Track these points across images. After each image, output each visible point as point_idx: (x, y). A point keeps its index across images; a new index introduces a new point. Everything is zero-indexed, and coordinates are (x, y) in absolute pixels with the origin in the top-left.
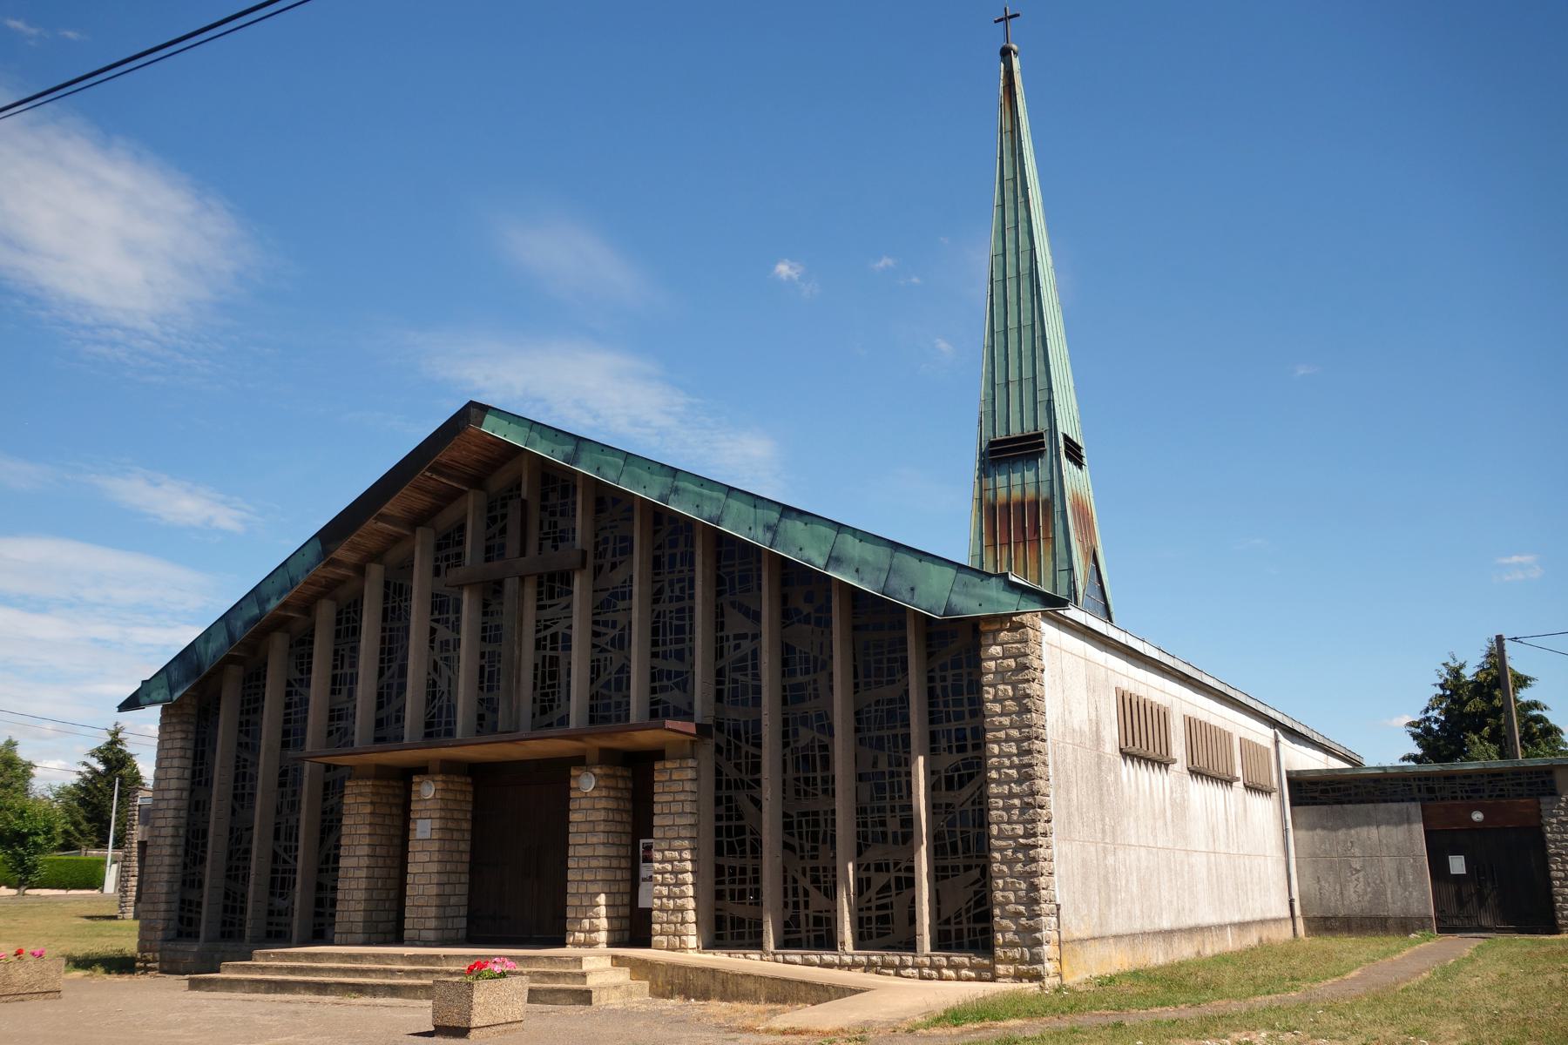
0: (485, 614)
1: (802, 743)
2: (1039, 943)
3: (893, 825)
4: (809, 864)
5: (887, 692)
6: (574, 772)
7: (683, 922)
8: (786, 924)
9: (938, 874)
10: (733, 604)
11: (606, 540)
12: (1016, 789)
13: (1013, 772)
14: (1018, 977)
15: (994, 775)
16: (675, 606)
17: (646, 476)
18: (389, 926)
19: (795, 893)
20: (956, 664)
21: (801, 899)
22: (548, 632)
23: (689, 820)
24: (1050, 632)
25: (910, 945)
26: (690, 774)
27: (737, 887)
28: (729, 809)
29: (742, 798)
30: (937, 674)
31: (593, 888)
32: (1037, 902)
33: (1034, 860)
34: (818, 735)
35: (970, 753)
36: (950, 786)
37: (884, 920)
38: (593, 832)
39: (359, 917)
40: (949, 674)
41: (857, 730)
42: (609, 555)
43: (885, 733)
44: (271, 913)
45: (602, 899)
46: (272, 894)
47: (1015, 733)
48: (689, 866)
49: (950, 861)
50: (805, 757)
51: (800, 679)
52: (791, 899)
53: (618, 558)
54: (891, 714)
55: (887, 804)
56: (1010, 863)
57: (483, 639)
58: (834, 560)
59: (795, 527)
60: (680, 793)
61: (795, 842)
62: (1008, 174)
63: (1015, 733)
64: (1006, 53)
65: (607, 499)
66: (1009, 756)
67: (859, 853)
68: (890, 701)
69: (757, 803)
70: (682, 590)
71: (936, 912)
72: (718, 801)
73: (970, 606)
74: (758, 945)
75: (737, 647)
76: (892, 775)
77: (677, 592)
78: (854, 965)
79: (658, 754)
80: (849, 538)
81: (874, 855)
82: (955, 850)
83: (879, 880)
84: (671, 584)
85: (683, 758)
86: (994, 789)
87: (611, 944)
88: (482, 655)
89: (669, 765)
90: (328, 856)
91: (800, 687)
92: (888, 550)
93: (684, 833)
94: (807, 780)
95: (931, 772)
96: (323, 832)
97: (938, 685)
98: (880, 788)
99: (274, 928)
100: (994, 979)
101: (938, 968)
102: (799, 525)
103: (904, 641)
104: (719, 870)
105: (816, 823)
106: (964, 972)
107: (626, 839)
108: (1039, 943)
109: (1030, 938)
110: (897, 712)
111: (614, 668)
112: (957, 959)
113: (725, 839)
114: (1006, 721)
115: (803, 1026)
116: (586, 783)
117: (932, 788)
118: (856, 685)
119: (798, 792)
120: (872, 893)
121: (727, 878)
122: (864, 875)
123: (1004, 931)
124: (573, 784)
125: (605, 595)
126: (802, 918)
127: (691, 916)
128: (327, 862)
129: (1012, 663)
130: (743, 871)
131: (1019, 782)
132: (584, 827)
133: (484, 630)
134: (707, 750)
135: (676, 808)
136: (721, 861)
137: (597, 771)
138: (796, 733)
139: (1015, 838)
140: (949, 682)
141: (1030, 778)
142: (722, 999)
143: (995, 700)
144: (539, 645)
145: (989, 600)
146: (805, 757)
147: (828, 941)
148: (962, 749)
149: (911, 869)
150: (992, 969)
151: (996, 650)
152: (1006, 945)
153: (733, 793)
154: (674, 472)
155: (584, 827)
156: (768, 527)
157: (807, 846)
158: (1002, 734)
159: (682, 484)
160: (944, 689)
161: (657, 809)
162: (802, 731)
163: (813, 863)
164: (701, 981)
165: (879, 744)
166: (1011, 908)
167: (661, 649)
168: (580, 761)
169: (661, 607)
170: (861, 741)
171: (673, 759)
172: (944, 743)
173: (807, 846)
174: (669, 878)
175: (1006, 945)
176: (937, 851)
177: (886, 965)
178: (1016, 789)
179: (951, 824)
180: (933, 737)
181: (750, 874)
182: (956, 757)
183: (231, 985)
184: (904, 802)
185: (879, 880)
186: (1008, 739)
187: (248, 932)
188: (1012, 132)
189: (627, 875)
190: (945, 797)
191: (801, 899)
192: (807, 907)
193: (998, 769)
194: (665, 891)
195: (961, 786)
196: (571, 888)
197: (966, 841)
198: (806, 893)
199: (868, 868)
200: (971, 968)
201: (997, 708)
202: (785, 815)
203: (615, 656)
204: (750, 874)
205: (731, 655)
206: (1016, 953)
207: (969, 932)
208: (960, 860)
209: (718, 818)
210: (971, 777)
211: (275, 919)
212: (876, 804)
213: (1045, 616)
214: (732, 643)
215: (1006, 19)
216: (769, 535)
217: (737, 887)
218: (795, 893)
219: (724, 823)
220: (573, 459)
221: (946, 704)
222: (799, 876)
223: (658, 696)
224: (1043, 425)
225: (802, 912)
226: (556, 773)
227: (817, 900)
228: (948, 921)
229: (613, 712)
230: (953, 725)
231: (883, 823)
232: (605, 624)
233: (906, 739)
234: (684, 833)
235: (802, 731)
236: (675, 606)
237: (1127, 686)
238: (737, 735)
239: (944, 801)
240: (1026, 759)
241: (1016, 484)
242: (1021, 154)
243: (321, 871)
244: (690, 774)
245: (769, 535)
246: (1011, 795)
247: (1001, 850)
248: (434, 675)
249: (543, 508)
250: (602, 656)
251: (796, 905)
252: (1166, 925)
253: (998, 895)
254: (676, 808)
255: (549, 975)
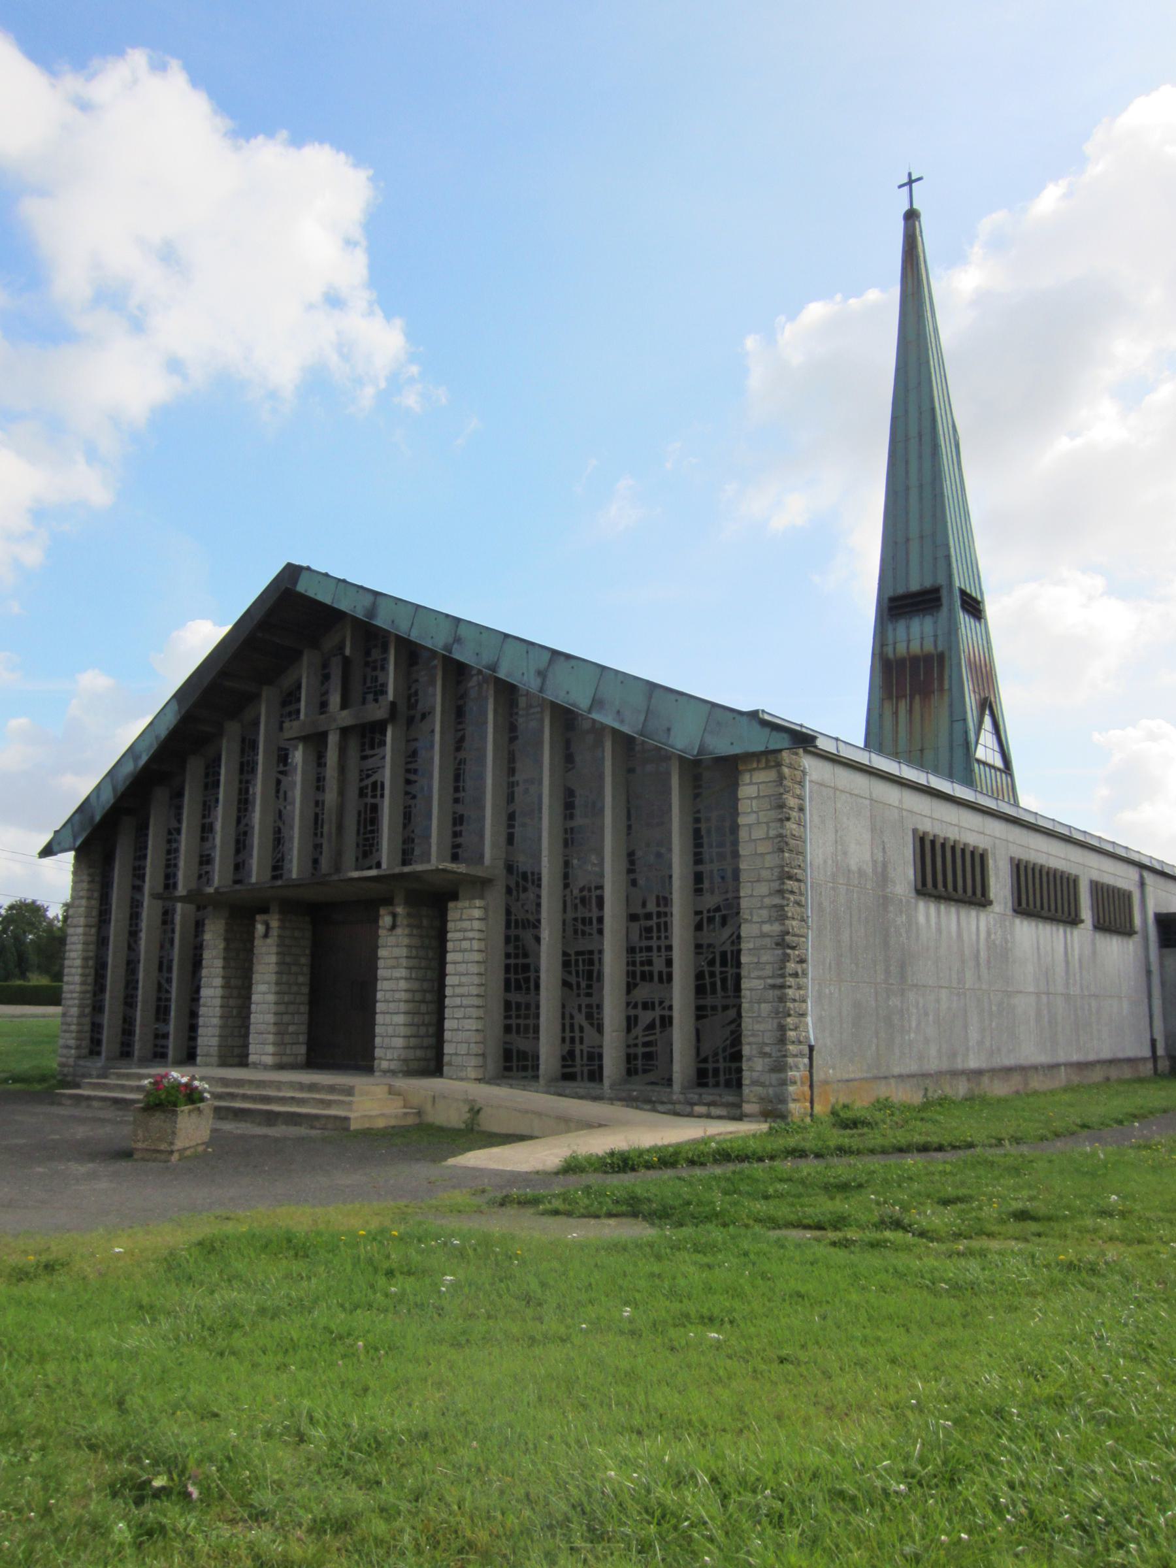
4: (585, 1001)
19: (572, 1030)
23: (477, 957)
26: (477, 913)
28: (516, 947)
29: (527, 936)
37: (648, 1056)
49: (709, 1001)
52: (568, 1034)
55: (654, 943)
60: (471, 933)
61: (573, 980)
69: (538, 939)
72: (508, 940)
76: (659, 915)
82: (714, 992)
83: (646, 1017)
104: (508, 1005)
119: (576, 932)
120: (638, 1031)
121: (513, 1013)
122: (632, 1012)
126: (578, 1052)
144: (362, 793)
157: (583, 984)
173: (583, 984)
179: (711, 963)
185: (646, 1017)
191: (577, 1034)
192: (581, 1042)
197: (724, 981)
198: (581, 1029)
202: (565, 954)
207: (719, 1074)
209: (508, 956)
212: (644, 943)
218: (572, 1030)
222: (575, 1012)
224: (941, 580)
228: (705, 1060)
231: (650, 963)
237: (926, 826)
239: (705, 942)
241: (917, 634)
244: (477, 913)
245: (539, 681)
251: (572, 1040)
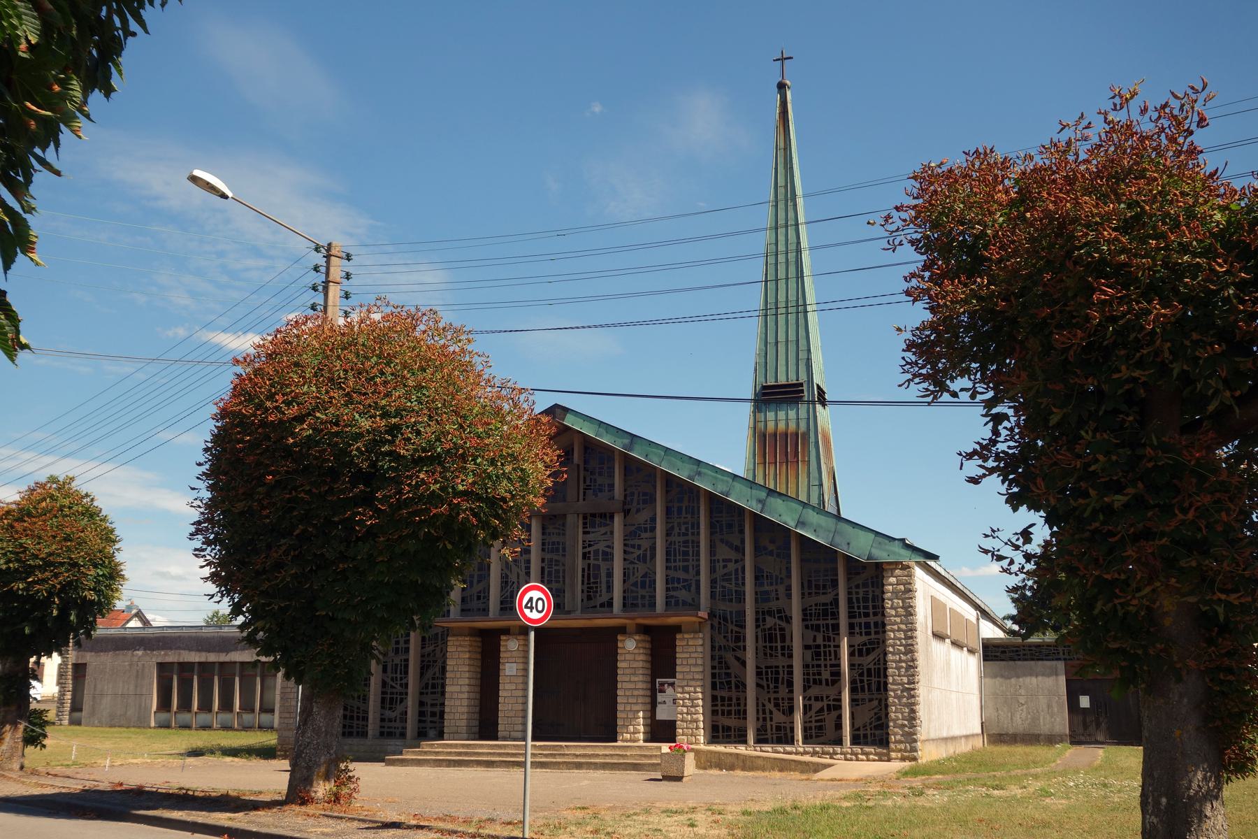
0: (543, 534)
1: (768, 626)
2: (915, 741)
3: (826, 675)
4: (773, 696)
5: (823, 599)
6: (620, 637)
7: (697, 728)
8: (758, 730)
9: (853, 701)
10: (722, 541)
11: (632, 494)
12: (903, 657)
13: (902, 648)
14: (903, 759)
15: (891, 649)
16: (682, 539)
17: (679, 463)
18: (486, 726)
19: (764, 713)
20: (865, 585)
21: (768, 716)
22: (591, 549)
23: (701, 669)
24: (919, 573)
25: (839, 742)
26: (700, 642)
27: (726, 708)
28: (720, 663)
29: (729, 657)
30: (854, 590)
31: (635, 708)
32: (914, 719)
33: (913, 696)
34: (778, 622)
35: (873, 636)
36: (861, 654)
37: (820, 728)
38: (634, 674)
39: (464, 723)
40: (861, 591)
41: (803, 620)
42: (635, 504)
43: (821, 622)
44: (382, 720)
45: (641, 714)
46: (383, 708)
47: (903, 627)
48: (700, 695)
49: (860, 696)
50: (770, 635)
51: (766, 588)
52: (761, 716)
53: (641, 506)
54: (825, 613)
55: (822, 663)
56: (899, 698)
57: (543, 550)
58: (801, 523)
59: (777, 503)
60: (692, 654)
61: (764, 683)
62: (781, 182)
63: (903, 627)
64: (782, 87)
65: (633, 468)
66: (900, 639)
67: (805, 690)
68: (824, 604)
70: (687, 529)
71: (852, 725)
72: (713, 658)
73: (882, 555)
74: (745, 742)
75: (725, 567)
76: (825, 646)
77: (683, 530)
78: (805, 753)
79: (677, 629)
80: (810, 511)
81: (815, 691)
82: (863, 689)
83: (817, 706)
84: (679, 524)
85: (695, 632)
86: (890, 657)
87: (645, 741)
88: (543, 560)
89: (686, 636)
90: (427, 684)
91: (767, 593)
92: (834, 520)
93: (697, 676)
94: (771, 648)
95: (850, 646)
96: (422, 668)
97: (854, 596)
98: (818, 654)
99: (386, 730)
100: (889, 760)
101: (856, 755)
102: (779, 501)
103: (836, 569)
104: (714, 698)
105: (777, 673)
106: (871, 757)
107: (649, 679)
108: (915, 741)
109: (911, 738)
110: (830, 611)
111: (640, 574)
112: (867, 749)
113: (717, 680)
114: (898, 620)
115: (838, 777)
116: (630, 647)
117: (851, 654)
118: (803, 594)
119: (765, 654)
120: (812, 713)
121: (719, 703)
122: (808, 703)
123: (895, 734)
124: (620, 645)
125: (633, 528)
126: (769, 727)
127: (701, 725)
128: (427, 688)
129: (902, 587)
130: (730, 699)
131: (905, 654)
132: (627, 671)
133: (543, 544)
134: (707, 628)
135: (691, 661)
136: (716, 693)
137: (637, 637)
138: (764, 620)
139: (902, 684)
140: (861, 596)
141: (912, 652)
142: (743, 769)
143: (892, 608)
144: (585, 556)
145: (894, 553)
146: (770, 635)
147: (791, 741)
148: (868, 634)
149: (840, 700)
150: (888, 755)
151: (893, 580)
152: (896, 742)
153: (722, 653)
154: (699, 462)
155: (627, 671)
156: (760, 501)
157: (772, 686)
158: (896, 627)
159: (703, 470)
160: (858, 599)
161: (678, 662)
162: (768, 619)
163: (775, 695)
164: (730, 760)
165: (817, 628)
166: (900, 722)
167: (673, 564)
168: (622, 630)
169: (672, 539)
170: (807, 627)
171: (687, 632)
172: (857, 629)
173: (772, 686)
174: (688, 703)
175: (896, 742)
176: (853, 690)
177: (824, 753)
178: (903, 657)
179: (861, 675)
180: (851, 626)
181: (734, 701)
182: (864, 638)
183: (404, 762)
184: (833, 662)
185: (817, 706)
186: (899, 630)
187: (370, 733)
188: (785, 149)
189: (648, 700)
190: (857, 660)
191: (768, 716)
192: (771, 719)
193: (893, 646)
194: (685, 710)
195: (868, 654)
196: (620, 707)
197: (869, 685)
198: (771, 713)
199: (810, 699)
200: (876, 754)
201: (893, 612)
202: (757, 667)
203: (642, 568)
204: (734, 701)
205: (720, 572)
206: (902, 746)
207: (875, 733)
208: (866, 695)
209: (713, 668)
210: (874, 649)
211: (386, 724)
212: (815, 662)
213: (918, 563)
214: (722, 564)
215: (783, 59)
216: (760, 506)
217: (726, 708)
218: (764, 713)
219: (717, 671)
220: (630, 448)
221: (859, 607)
222: (766, 703)
223: (671, 593)
224: (803, 378)
225: (769, 723)
226: (610, 637)
227: (779, 717)
228: (858, 729)
229: (639, 601)
230: (863, 620)
231: (819, 674)
232: (633, 546)
233: (836, 627)
234: (697, 676)
235: (768, 619)
236: (682, 539)
237: (938, 596)
238: (725, 619)
239: (857, 663)
240: (910, 641)
241: (783, 419)
242: (792, 168)
243: (421, 693)
244: (700, 642)
245: (760, 506)
246: (901, 661)
247: (894, 691)
248: (506, 571)
249: (585, 469)
250: (631, 566)
251: (765, 719)
252: (945, 735)
253: (892, 715)
254: (691, 661)
255: (645, 756)
